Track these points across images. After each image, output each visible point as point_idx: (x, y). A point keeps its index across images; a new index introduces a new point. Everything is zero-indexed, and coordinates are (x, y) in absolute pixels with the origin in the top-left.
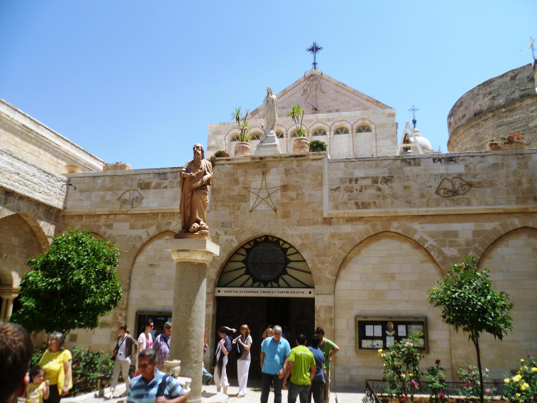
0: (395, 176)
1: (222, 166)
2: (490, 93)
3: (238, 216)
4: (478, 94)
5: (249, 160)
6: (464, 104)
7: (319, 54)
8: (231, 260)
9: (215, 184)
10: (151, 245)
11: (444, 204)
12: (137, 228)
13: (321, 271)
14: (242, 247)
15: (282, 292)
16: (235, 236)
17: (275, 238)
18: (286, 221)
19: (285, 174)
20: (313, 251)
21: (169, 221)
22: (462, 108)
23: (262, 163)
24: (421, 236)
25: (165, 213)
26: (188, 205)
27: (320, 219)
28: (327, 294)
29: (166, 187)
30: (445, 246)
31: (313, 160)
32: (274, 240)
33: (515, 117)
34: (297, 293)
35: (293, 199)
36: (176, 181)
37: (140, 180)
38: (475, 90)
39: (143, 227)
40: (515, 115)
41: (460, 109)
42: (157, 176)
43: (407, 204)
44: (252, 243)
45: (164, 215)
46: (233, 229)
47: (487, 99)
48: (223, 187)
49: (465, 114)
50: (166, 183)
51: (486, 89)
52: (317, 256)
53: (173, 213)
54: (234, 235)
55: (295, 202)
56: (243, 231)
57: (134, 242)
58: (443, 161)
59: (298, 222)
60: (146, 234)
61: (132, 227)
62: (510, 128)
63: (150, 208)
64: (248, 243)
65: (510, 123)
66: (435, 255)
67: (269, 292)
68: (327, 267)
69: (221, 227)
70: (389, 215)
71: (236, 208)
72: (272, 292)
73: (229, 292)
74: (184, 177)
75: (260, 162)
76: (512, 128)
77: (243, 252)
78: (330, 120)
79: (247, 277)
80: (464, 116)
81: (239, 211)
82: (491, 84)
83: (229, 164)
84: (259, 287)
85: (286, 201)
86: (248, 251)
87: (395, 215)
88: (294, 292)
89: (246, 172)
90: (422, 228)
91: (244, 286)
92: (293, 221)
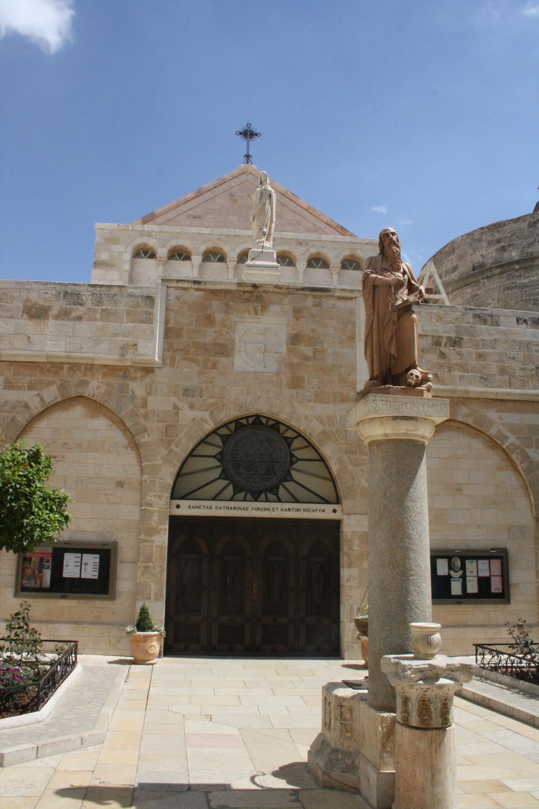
0: (466, 338)
1: (184, 292)
2: (499, 241)
3: (213, 378)
4: (480, 240)
5: (234, 287)
6: (456, 251)
7: (255, 143)
8: (193, 453)
9: (172, 321)
10: (46, 420)
11: (531, 385)
12: (19, 388)
13: (353, 477)
14: (215, 432)
15: (289, 510)
16: (208, 413)
17: (231, 422)
18: (297, 393)
19: (294, 317)
20: (340, 444)
21: (84, 379)
22: (453, 257)
23: (255, 294)
24: (500, 430)
25: (74, 364)
26: (392, 336)
27: (352, 394)
28: (363, 514)
29: (80, 318)
30: (531, 447)
31: (340, 298)
32: (271, 423)
33: (532, 279)
34: (313, 511)
35: (307, 359)
36: (99, 308)
37: (28, 300)
38: (476, 234)
39: (31, 387)
40: (532, 276)
41: (450, 258)
42: (62, 297)
43: (482, 380)
44: (232, 426)
45: (74, 367)
46: (204, 400)
47: (493, 249)
48: (186, 328)
49: (457, 265)
50: (80, 311)
51: (493, 235)
52: (346, 452)
53: (92, 366)
54: (207, 410)
55: (311, 363)
56: (223, 405)
57: (14, 414)
58: (529, 322)
59: (317, 396)
60: (38, 399)
61: (9, 385)
62: (525, 292)
63: (49, 353)
64: (226, 425)
65: (525, 286)
66: (518, 458)
67: (266, 509)
68: (363, 470)
69: (183, 395)
70: (456, 395)
71: (209, 365)
72: (271, 509)
73: (197, 507)
74: (376, 283)
75: (251, 292)
76: (528, 293)
77: (218, 441)
78: (303, 244)
79: (224, 483)
80: (455, 269)
81: (216, 371)
82: (500, 229)
83: (196, 290)
84: (245, 500)
85: (296, 360)
86: (225, 439)
87: (465, 395)
88: (308, 510)
89: (227, 305)
90: (500, 418)
91: (218, 498)
92: (308, 393)
